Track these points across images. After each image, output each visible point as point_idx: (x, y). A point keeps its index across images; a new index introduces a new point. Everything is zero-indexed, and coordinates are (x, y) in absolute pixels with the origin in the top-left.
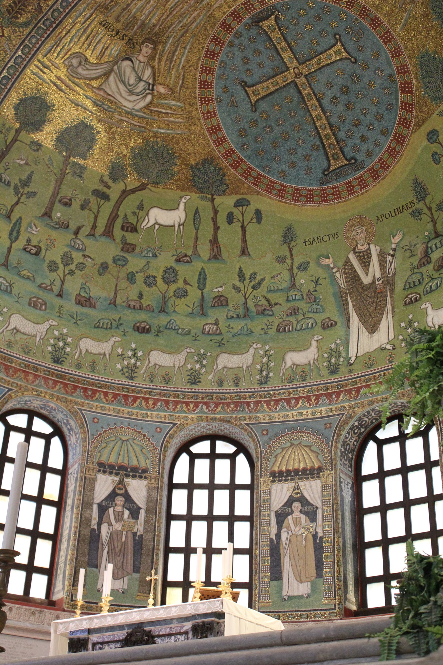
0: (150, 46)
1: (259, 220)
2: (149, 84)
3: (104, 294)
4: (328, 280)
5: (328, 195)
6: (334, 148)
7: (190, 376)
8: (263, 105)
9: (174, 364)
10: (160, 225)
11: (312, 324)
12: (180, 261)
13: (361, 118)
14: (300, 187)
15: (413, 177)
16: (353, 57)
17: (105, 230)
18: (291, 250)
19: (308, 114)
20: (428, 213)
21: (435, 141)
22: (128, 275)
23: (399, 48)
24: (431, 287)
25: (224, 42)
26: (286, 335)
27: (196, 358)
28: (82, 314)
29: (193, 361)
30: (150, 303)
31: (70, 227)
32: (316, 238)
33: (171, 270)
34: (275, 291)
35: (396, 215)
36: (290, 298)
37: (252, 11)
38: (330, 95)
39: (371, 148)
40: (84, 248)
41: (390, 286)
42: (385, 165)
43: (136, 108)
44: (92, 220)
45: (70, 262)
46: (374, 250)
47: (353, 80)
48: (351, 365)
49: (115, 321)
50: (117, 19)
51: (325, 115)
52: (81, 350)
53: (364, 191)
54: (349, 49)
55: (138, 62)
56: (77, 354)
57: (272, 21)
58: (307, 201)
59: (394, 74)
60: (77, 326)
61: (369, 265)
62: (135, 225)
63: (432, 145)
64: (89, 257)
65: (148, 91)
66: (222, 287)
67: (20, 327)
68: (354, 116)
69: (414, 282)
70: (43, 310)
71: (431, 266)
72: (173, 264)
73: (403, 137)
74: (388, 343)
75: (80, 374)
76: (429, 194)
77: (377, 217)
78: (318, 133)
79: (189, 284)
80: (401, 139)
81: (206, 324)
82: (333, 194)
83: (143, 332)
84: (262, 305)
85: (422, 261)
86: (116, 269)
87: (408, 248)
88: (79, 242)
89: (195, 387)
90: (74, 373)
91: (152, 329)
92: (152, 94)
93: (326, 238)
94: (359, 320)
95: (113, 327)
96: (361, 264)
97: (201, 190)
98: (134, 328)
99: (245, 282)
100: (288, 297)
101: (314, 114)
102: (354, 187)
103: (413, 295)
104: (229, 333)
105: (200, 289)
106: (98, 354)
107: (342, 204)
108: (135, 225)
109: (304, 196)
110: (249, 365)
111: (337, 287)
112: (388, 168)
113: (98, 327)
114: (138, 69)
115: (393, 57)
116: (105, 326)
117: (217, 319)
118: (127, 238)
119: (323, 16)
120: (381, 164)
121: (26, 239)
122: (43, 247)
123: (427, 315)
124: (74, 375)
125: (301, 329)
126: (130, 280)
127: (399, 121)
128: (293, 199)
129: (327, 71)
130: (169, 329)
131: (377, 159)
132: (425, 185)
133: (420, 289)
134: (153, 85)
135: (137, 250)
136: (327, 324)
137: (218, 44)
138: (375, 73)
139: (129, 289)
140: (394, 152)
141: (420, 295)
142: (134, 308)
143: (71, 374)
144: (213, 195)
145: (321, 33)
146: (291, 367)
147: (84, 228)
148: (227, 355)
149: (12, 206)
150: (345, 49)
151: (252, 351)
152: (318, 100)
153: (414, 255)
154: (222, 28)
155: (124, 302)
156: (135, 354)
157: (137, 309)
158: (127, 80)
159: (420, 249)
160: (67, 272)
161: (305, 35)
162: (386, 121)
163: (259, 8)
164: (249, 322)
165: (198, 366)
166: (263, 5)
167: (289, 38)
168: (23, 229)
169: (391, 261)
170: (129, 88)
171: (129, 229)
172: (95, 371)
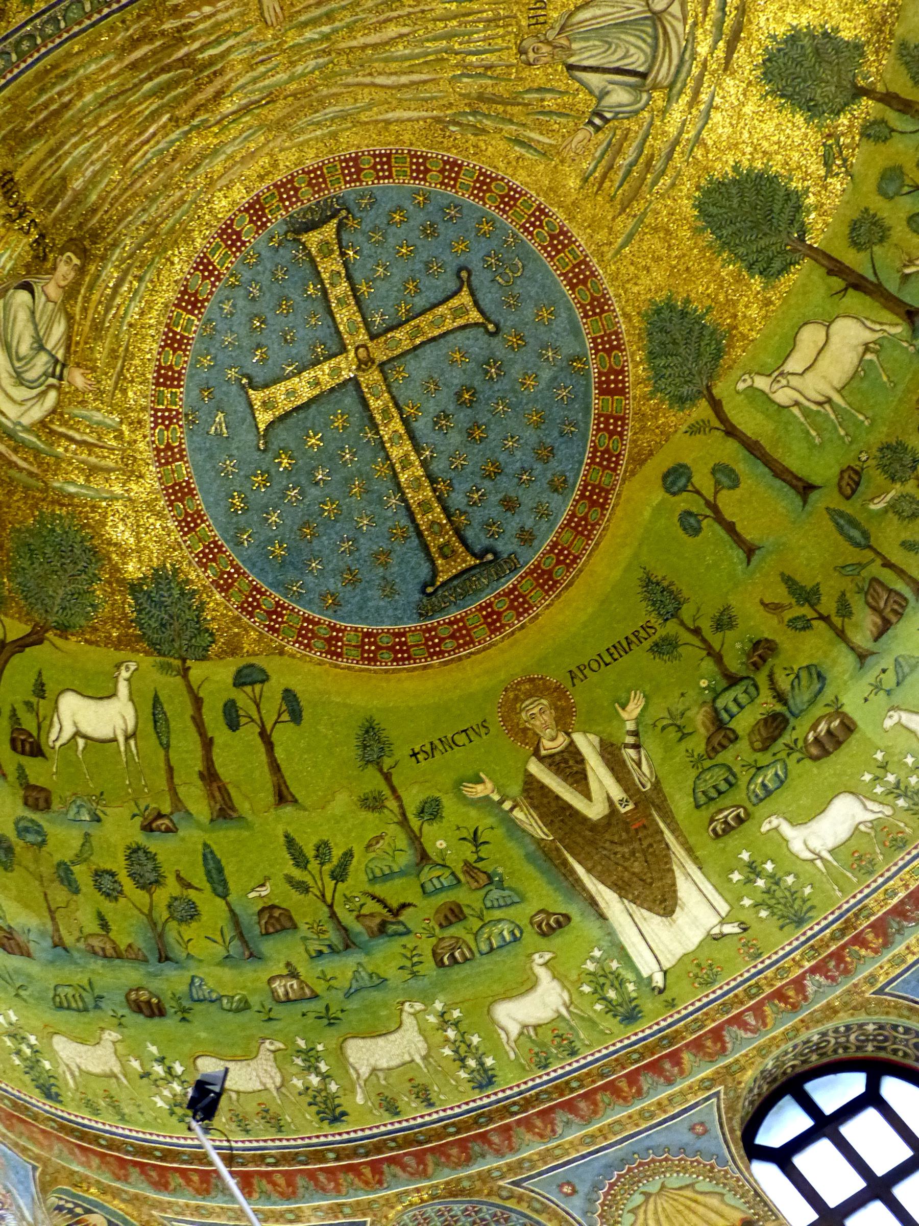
0: (76, 261)
1: (296, 716)
2: (57, 361)
4: (500, 831)
5: (442, 640)
6: (441, 532)
7: (315, 1104)
8: (282, 435)
9: (264, 1085)
10: (85, 737)
11: (512, 933)
12: (152, 830)
13: (502, 457)
14: (374, 628)
15: (640, 574)
16: (490, 322)
18: (387, 777)
19: (382, 454)
20: (696, 641)
21: (684, 489)
23: (604, 295)
24: (764, 785)
25: (220, 274)
26: (467, 969)
27: (299, 1061)
29: (294, 1070)
30: (129, 941)
32: (437, 742)
33: (141, 853)
34: (387, 877)
35: (615, 660)
36: (429, 888)
37: (292, 204)
38: (432, 408)
39: (529, 523)
41: (659, 809)
42: (567, 557)
43: (26, 421)
46: (586, 744)
47: (487, 372)
48: (661, 991)
50: (31, 176)
51: (419, 454)
52: (67, 1066)
53: (525, 619)
54: (485, 303)
55: (43, 298)
57: (329, 230)
58: (396, 660)
59: (586, 355)
61: (585, 778)
63: (676, 498)
65: (51, 381)
66: (263, 885)
68: (484, 455)
69: (714, 787)
71: (743, 745)
72: (141, 838)
73: (602, 489)
74: (723, 922)
76: (687, 600)
77: (570, 672)
78: (404, 500)
79: (189, 886)
80: (598, 495)
81: (271, 980)
82: (452, 636)
83: (152, 1015)
84: (372, 915)
85: (715, 742)
87: (665, 722)
89: (343, 1128)
91: (167, 1006)
92: (58, 388)
93: (461, 739)
94: (621, 897)
96: (565, 780)
97: (155, 648)
99: (309, 867)
100: (422, 886)
101: (396, 453)
102: (499, 614)
103: (726, 813)
104: (334, 992)
105: (219, 896)
107: (479, 656)
108: (35, 734)
109: (387, 648)
110: (423, 1053)
111: (528, 840)
112: (574, 561)
114: (41, 318)
115: (586, 316)
117: (288, 964)
119: (441, 228)
120: (558, 555)
123: (787, 841)
125: (492, 949)
127: (592, 458)
128: (363, 659)
129: (429, 354)
130: (199, 1001)
131: (545, 546)
132: (672, 583)
133: (739, 795)
134: (64, 366)
135: (56, 805)
136: (548, 924)
137: (208, 277)
138: (541, 355)
139: (73, 906)
140: (586, 525)
141: (745, 809)
142: (105, 956)
144: (184, 660)
145: (427, 265)
146: (521, 1034)
148: (360, 1042)
150: (476, 304)
151: (408, 1021)
152: (405, 422)
153: (690, 734)
154: (222, 240)
158: (14, 344)
159: (699, 718)
161: (394, 270)
162: (560, 462)
163: (309, 200)
164: (363, 959)
165: (315, 1080)
166: (318, 192)
167: (357, 276)
169: (635, 757)
170: (17, 365)
171: (27, 747)
172: (127, 1117)
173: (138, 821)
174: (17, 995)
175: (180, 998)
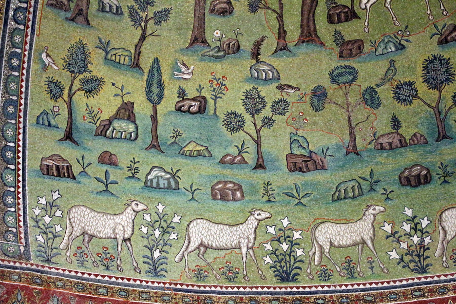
3: (334, 141)
12: (447, 42)
17: (302, 33)
22: (364, 94)
28: (305, 185)
30: (416, 130)
31: (242, 48)
33: (436, 62)
40: (275, 74)
44: (276, 23)
45: (261, 106)
49: (364, 179)
52: (321, 246)
56: (317, 255)
60: (302, 208)
62: (350, 6)
64: (289, 86)
67: (209, 240)
70: (239, 200)
72: (438, 51)
75: (332, 288)
86: (341, 92)
88: (265, 68)
90: (320, 289)
91: (434, 174)
95: (365, 191)
98: (401, 183)
106: (354, 245)
108: (350, 6)
113: (339, 199)
116: (351, 194)
118: (343, 33)
121: (176, 91)
122: (208, 97)
124: (322, 292)
126: (369, 102)
135: (367, 48)
139: (372, 118)
142: (391, 148)
143: (316, 293)
147: (266, 41)
149: (136, 46)
155: (370, 143)
156: (416, 225)
157: (397, 147)
160: (259, 124)
168: (165, 77)
172: (356, 275)
173: (436, 38)
174: (300, 203)
175: (446, 166)
